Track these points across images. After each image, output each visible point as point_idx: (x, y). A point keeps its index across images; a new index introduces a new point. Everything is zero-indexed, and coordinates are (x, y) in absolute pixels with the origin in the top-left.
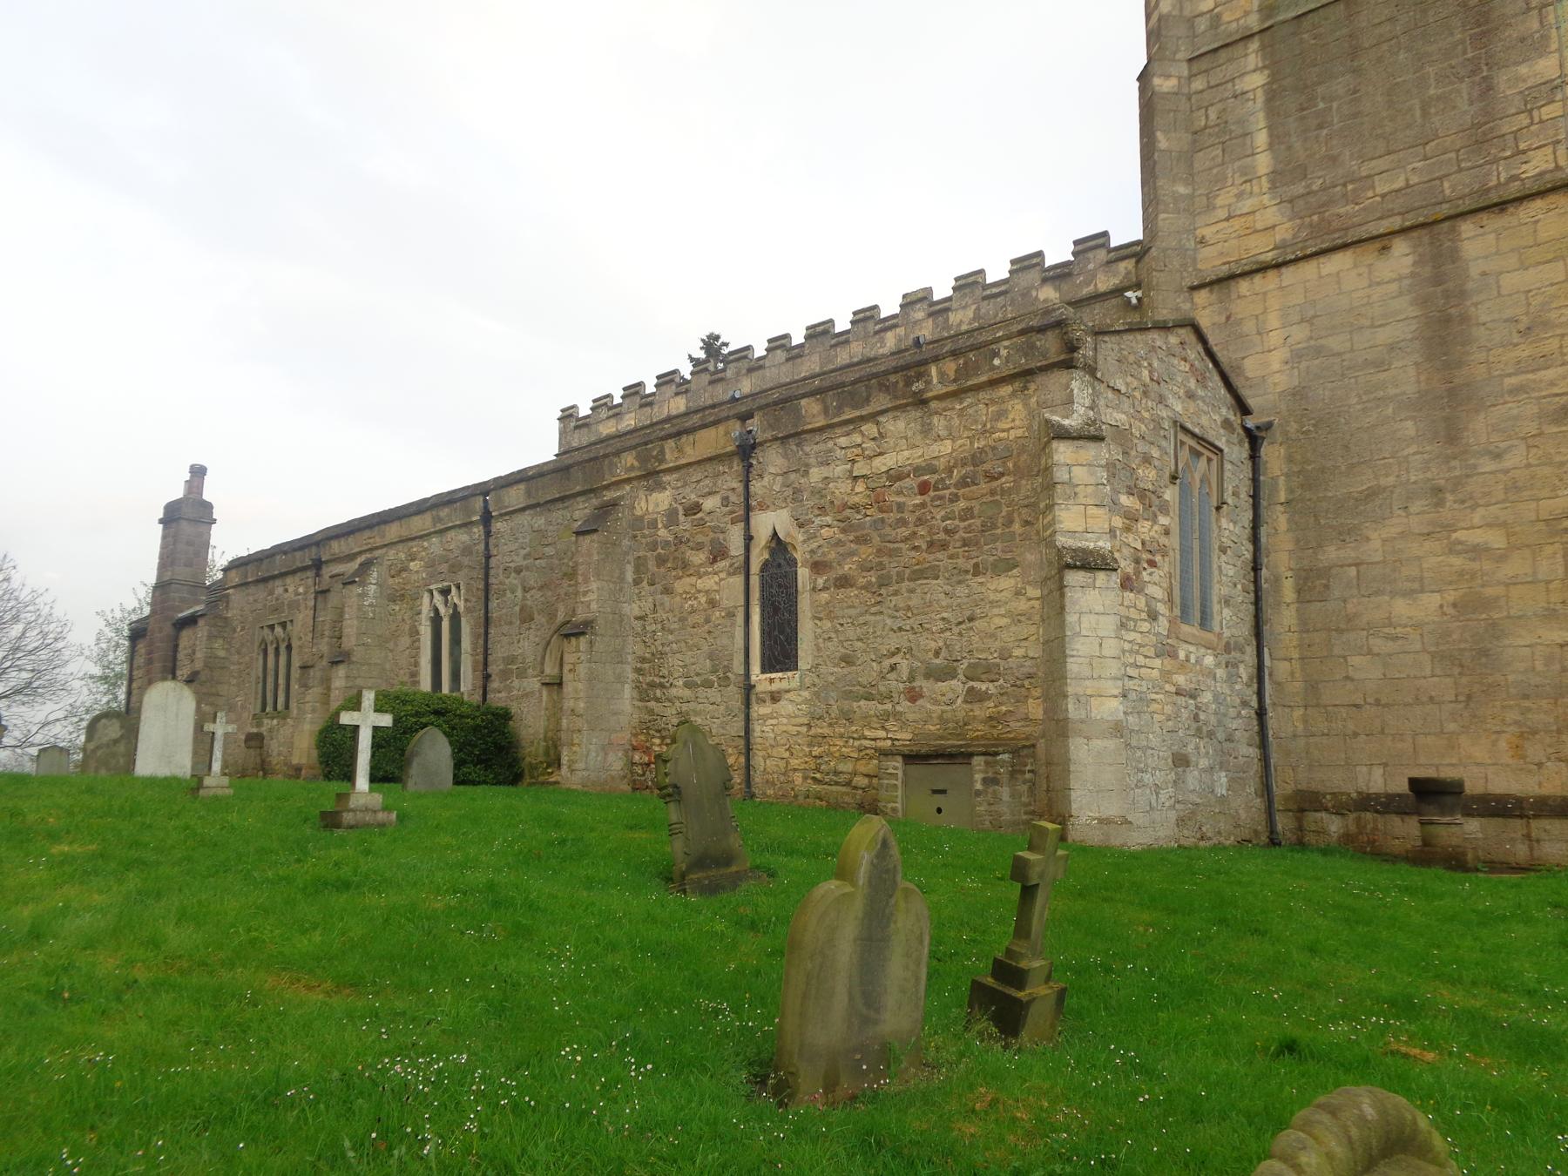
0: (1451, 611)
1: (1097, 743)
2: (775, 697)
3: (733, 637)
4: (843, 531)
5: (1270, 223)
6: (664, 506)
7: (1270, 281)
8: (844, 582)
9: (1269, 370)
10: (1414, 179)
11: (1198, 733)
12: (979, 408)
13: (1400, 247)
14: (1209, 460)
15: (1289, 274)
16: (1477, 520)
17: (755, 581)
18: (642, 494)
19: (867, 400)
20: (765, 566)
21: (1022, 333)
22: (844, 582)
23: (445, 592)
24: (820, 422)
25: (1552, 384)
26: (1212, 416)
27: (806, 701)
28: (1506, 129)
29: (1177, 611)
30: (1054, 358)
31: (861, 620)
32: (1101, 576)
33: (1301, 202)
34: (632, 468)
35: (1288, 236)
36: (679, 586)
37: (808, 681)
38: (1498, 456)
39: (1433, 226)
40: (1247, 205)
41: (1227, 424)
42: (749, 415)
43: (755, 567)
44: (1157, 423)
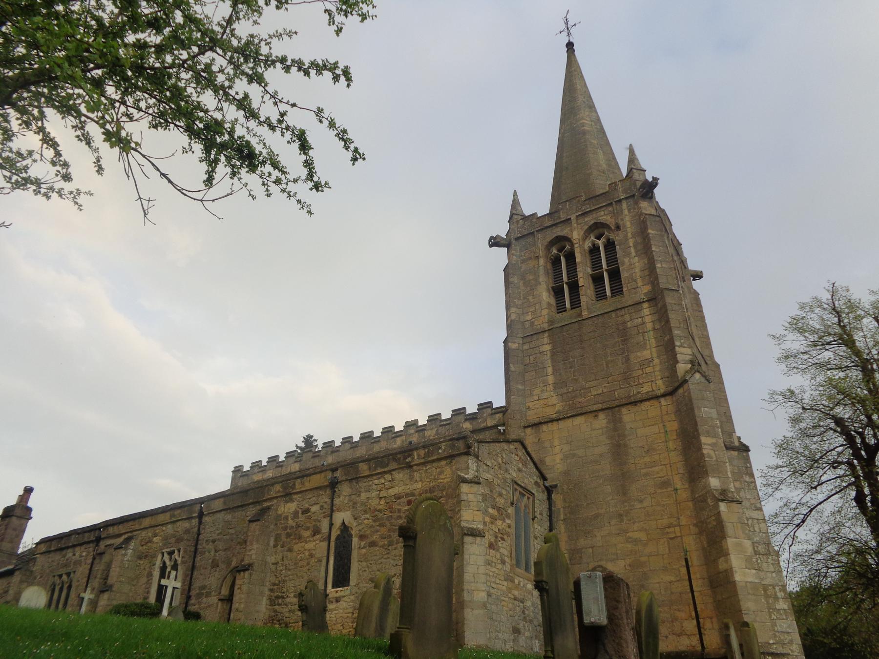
0: (628, 568)
1: (476, 612)
2: (338, 600)
3: (320, 571)
4: (374, 521)
5: (554, 403)
6: (293, 509)
7: (554, 426)
8: (373, 544)
9: (556, 464)
10: (605, 391)
11: (525, 619)
12: (433, 469)
13: (602, 416)
14: (528, 498)
15: (561, 423)
16: (636, 528)
17: (333, 544)
18: (282, 504)
19: (387, 465)
20: (338, 538)
21: (451, 440)
23: (171, 553)
24: (367, 473)
25: (658, 473)
26: (530, 479)
27: (352, 601)
28: (634, 375)
29: (514, 562)
30: (462, 451)
31: (380, 561)
32: (478, 539)
33: (565, 396)
34: (279, 491)
35: (561, 408)
36: (296, 548)
37: (354, 591)
38: (641, 501)
39: (612, 409)
40: (545, 395)
41: (536, 483)
42: (336, 470)
43: (333, 538)
44: (505, 480)
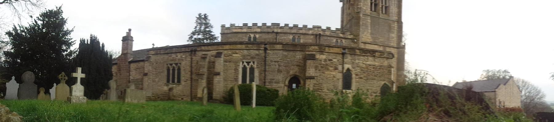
8: (361, 78)
22: (361, 78)
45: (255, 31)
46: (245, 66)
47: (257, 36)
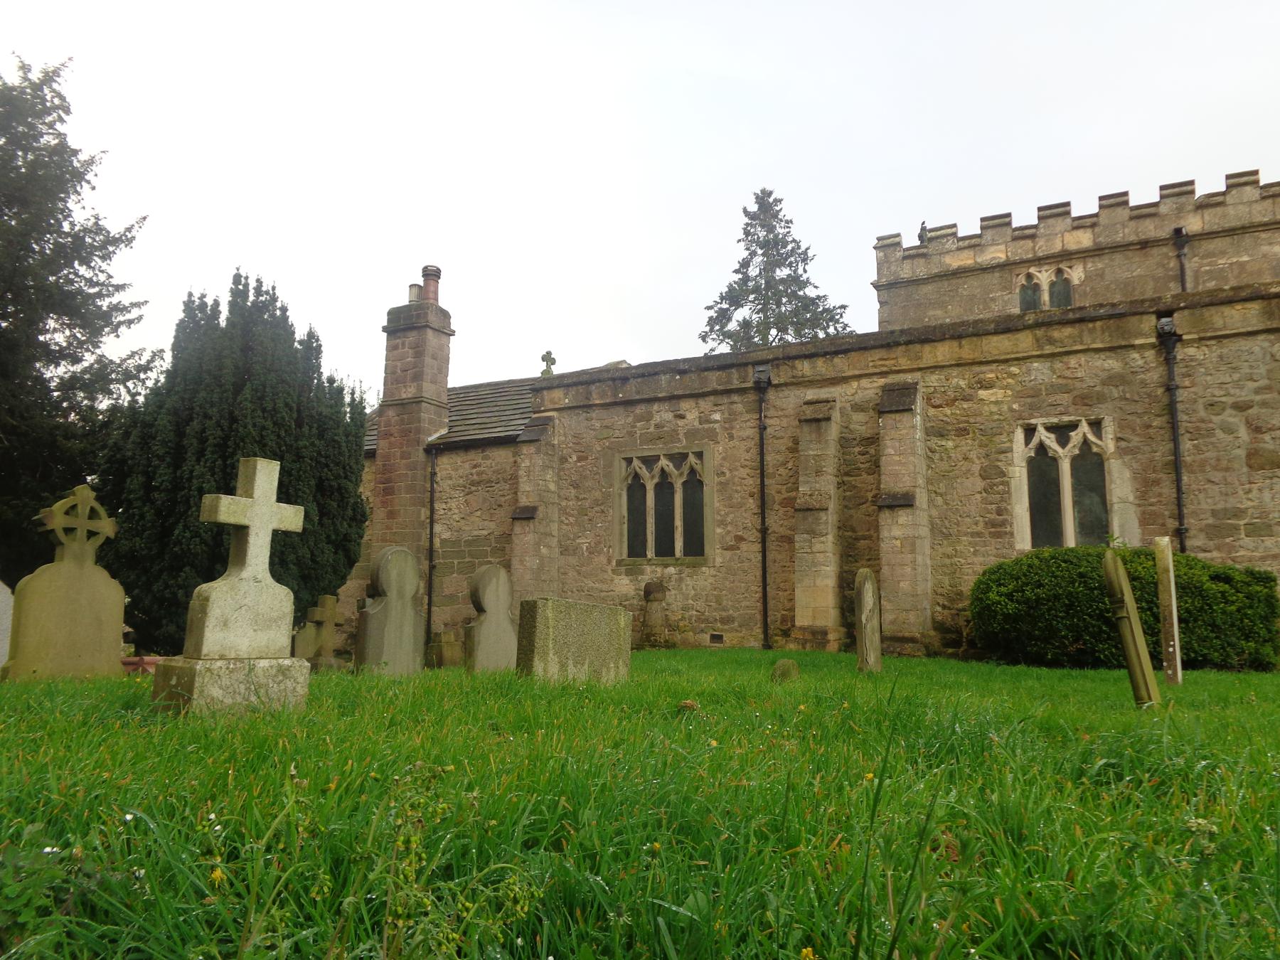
45: (1057, 247)
46: (1042, 448)
47: (1076, 274)
